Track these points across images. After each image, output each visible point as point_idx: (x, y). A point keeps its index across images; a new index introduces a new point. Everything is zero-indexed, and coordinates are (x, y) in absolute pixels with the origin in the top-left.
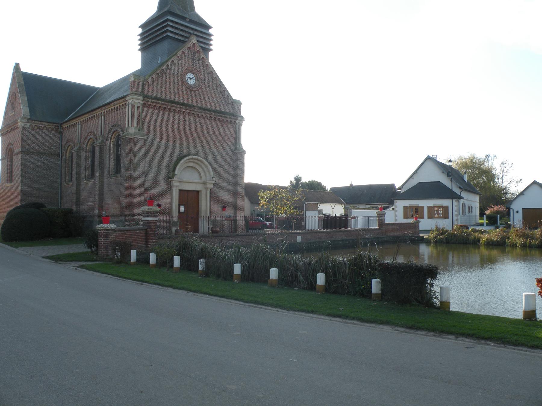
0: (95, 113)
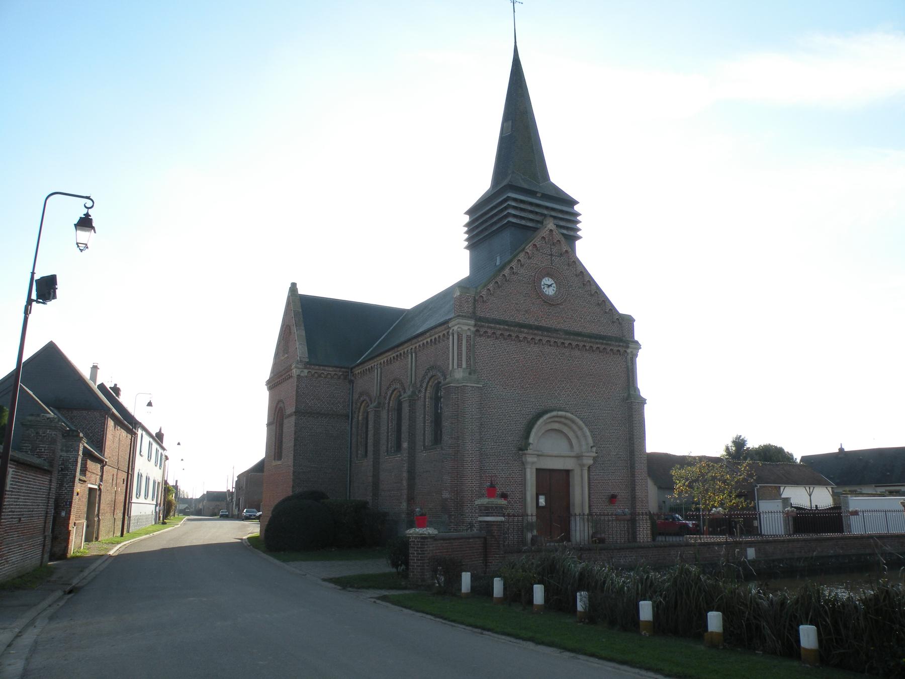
0: (401, 350)
